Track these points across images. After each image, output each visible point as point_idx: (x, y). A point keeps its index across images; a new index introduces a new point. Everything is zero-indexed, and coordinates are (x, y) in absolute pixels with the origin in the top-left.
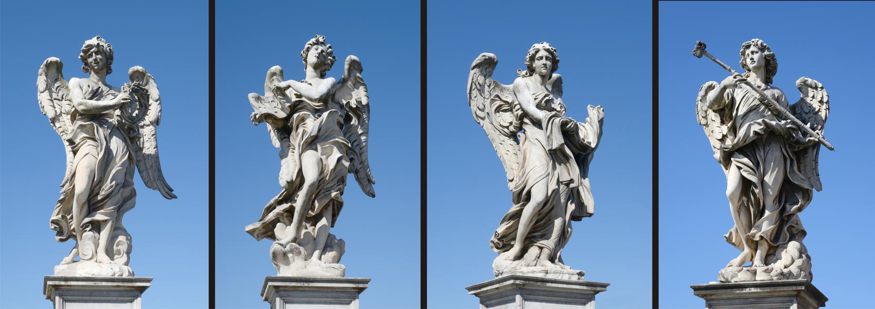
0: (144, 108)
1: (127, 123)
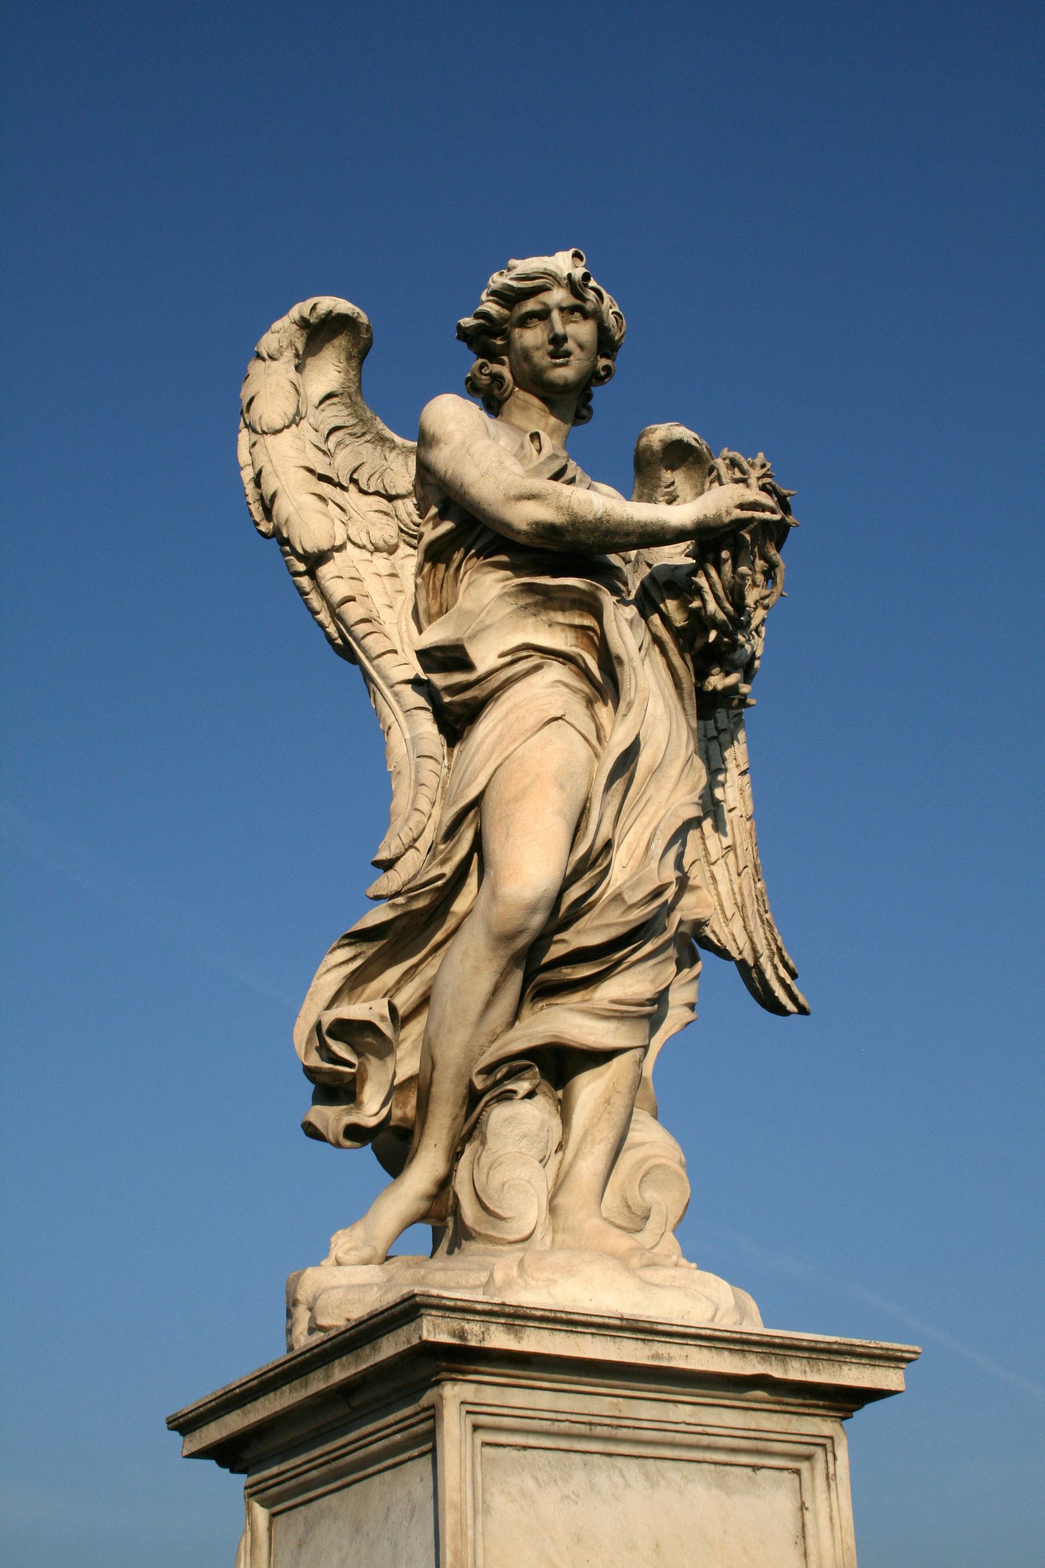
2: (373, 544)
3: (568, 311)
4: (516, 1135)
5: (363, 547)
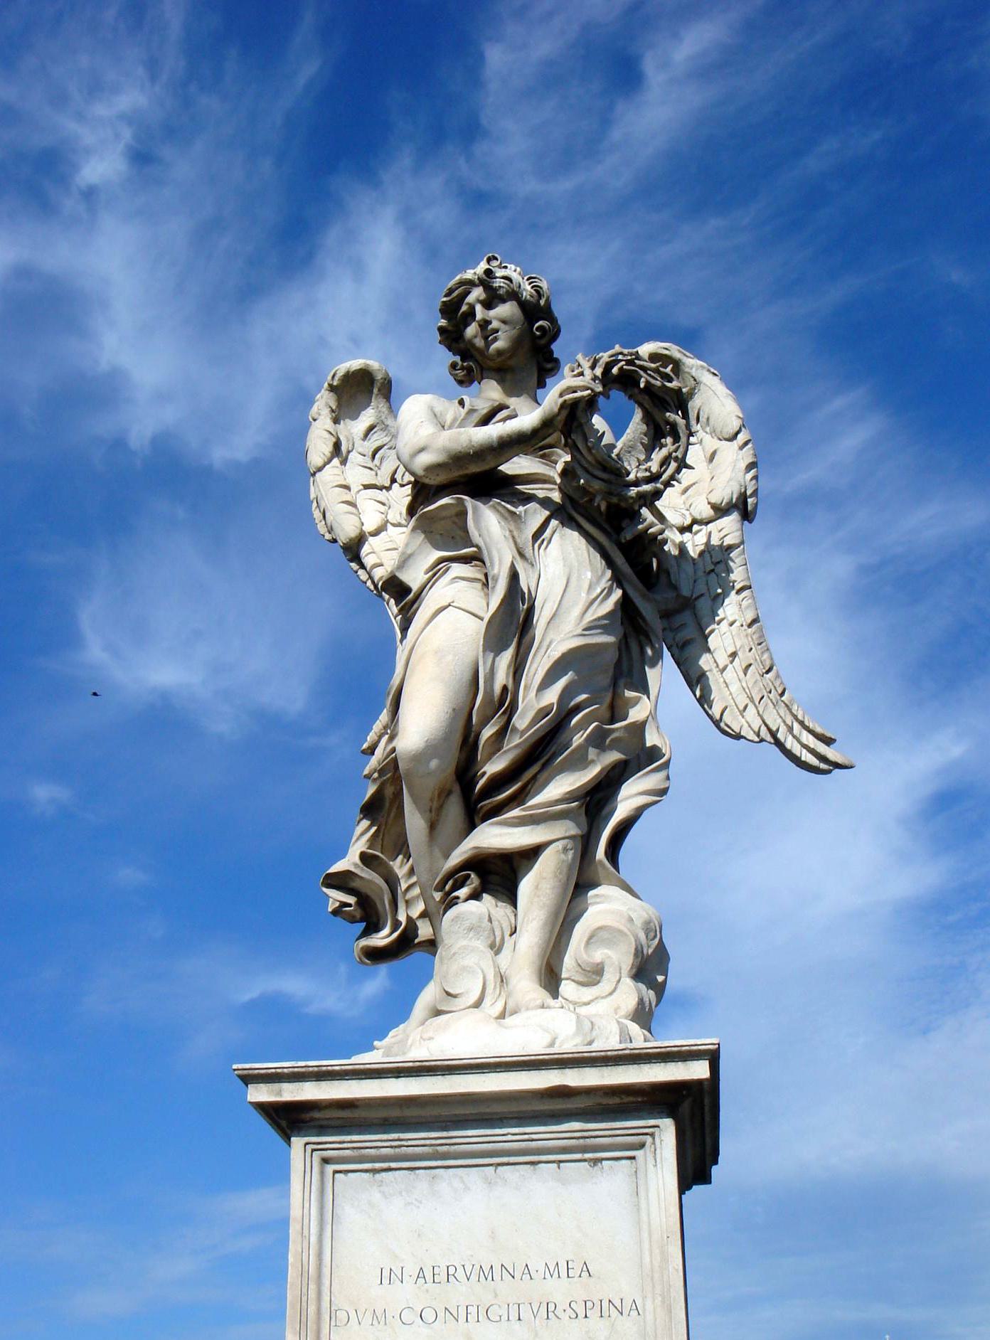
3: (488, 305)
4: (464, 930)
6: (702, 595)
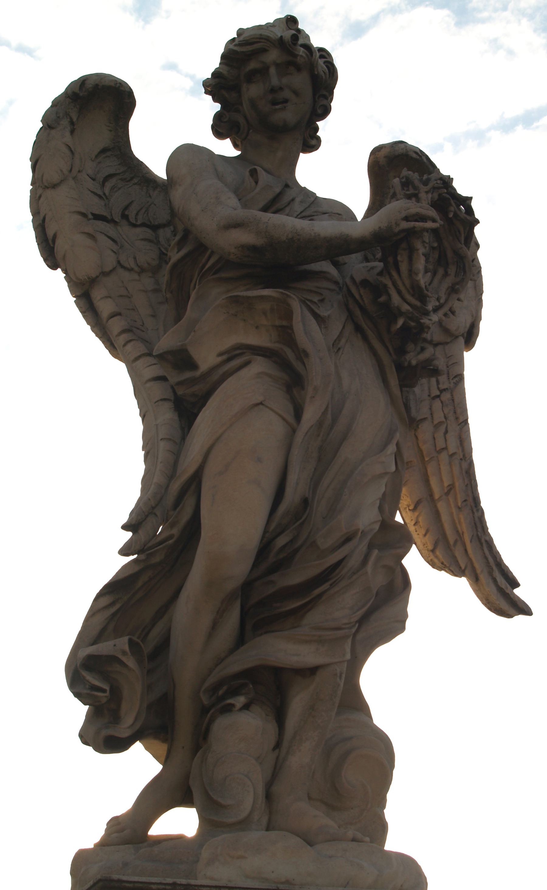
0: (452, 270)
1: (406, 307)
2: (139, 267)
5: (131, 270)
6: (425, 419)
